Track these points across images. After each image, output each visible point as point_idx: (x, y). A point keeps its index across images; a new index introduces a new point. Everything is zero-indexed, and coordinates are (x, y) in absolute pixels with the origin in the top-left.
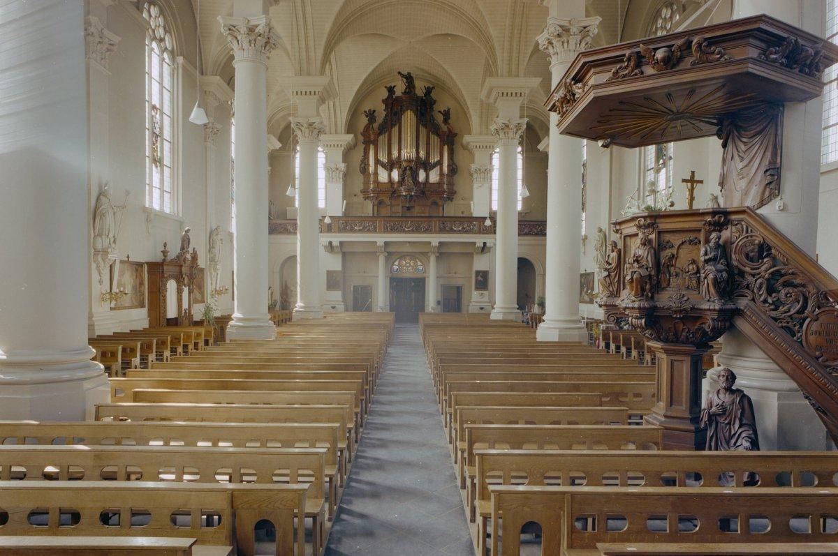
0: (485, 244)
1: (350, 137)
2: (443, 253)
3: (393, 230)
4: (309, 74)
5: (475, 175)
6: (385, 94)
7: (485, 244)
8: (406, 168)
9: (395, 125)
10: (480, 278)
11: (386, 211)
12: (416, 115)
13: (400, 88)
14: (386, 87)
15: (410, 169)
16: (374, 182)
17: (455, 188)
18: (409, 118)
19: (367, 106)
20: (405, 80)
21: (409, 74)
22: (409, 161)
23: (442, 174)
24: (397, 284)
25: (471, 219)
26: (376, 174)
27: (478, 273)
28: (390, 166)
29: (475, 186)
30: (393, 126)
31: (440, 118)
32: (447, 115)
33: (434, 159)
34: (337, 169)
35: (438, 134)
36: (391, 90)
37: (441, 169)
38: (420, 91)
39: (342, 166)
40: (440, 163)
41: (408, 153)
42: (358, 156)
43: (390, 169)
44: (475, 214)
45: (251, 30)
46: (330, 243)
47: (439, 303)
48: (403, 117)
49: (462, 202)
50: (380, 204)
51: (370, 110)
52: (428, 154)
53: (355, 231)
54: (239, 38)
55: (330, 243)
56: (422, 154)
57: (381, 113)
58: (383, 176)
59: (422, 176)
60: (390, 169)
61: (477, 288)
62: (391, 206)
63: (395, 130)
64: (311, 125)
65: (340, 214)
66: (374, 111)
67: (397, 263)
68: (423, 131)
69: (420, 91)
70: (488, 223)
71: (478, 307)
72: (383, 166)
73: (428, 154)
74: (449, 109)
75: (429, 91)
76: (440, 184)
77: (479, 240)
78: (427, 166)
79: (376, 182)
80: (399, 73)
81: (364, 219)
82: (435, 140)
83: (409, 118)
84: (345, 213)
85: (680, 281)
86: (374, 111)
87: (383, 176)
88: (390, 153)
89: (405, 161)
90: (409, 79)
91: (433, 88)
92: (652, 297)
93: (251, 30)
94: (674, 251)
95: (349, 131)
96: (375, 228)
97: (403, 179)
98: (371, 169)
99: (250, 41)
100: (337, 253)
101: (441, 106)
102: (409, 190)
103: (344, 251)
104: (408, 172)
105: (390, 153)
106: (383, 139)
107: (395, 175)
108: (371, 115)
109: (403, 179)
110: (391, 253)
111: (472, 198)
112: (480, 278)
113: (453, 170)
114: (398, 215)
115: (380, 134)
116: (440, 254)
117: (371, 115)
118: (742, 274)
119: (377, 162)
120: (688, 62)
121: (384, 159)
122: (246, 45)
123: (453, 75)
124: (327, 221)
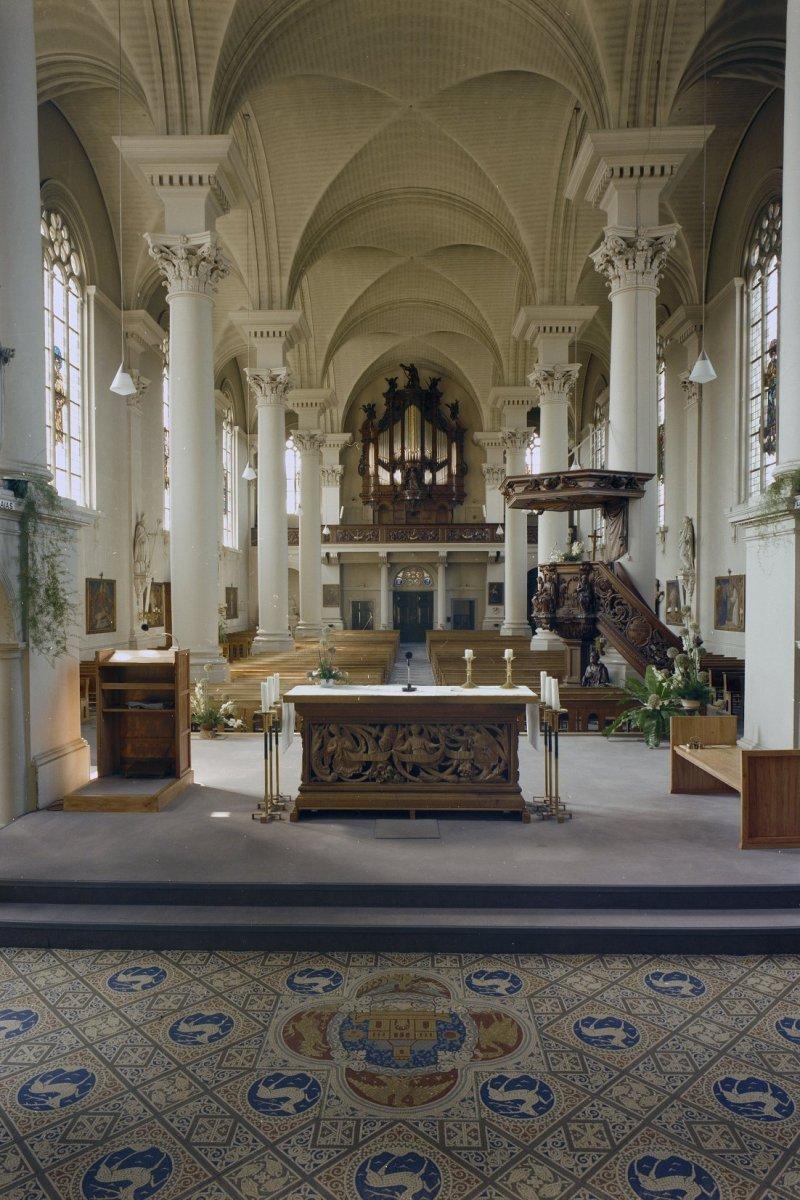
0: (498, 553)
1: (347, 436)
2: (452, 563)
3: (397, 539)
4: (311, 387)
5: (487, 476)
6: (386, 387)
7: (498, 553)
8: (410, 469)
9: (397, 421)
10: (494, 591)
11: (388, 518)
12: (421, 410)
13: (402, 381)
14: (387, 379)
15: (414, 470)
16: (375, 485)
17: (465, 491)
18: (412, 413)
19: (365, 401)
20: (408, 372)
21: (412, 365)
22: (413, 461)
23: (450, 475)
24: (402, 600)
25: (483, 526)
26: (376, 476)
27: (492, 585)
28: (392, 467)
29: (488, 487)
30: (395, 421)
31: (448, 412)
32: (455, 408)
33: (441, 457)
34: (334, 471)
35: (445, 431)
36: (392, 383)
37: (450, 469)
38: (425, 377)
39: (339, 468)
40: (448, 462)
41: (412, 452)
42: (355, 457)
43: (392, 472)
44: (488, 521)
45: (273, 379)
46: (328, 554)
47: (448, 619)
48: (406, 412)
49: (473, 505)
50: (381, 509)
51: (369, 405)
52: (434, 453)
53: (356, 541)
54: (262, 385)
55: (328, 554)
56: (428, 453)
57: (382, 408)
58: (384, 477)
59: (428, 477)
60: (392, 472)
61: (491, 603)
62: (394, 511)
63: (397, 428)
64: (312, 437)
65: (338, 523)
66: (374, 405)
67: (401, 574)
68: (428, 427)
69: (424, 384)
70: (499, 531)
71: (492, 624)
72: (385, 467)
73: (434, 453)
74: (457, 403)
75: (434, 382)
76: (447, 486)
77: (491, 549)
78: (434, 467)
79: (377, 484)
80: (402, 365)
81: (363, 528)
82: (441, 436)
83: (412, 413)
84: (341, 520)
85: (569, 602)
86: (374, 405)
87: (384, 477)
88: (392, 453)
89: (408, 461)
90: (412, 371)
91: (439, 379)
92: (554, 611)
93: (273, 379)
94: (566, 585)
95: (346, 429)
96: (377, 537)
97: (407, 482)
98: (372, 470)
99: (272, 389)
100: (335, 565)
101: (449, 399)
102: (414, 494)
103: (343, 564)
104: (412, 474)
105: (392, 453)
106: (384, 436)
107: (398, 476)
108: (370, 410)
109: (407, 482)
110: (393, 564)
111: (484, 502)
112: (494, 591)
113: (463, 469)
114: (401, 522)
115: (381, 431)
116: (449, 564)
117: (370, 410)
118: (599, 598)
119: (378, 462)
120: (559, 487)
121: (384, 456)
122: (268, 392)
123: (461, 367)
124: (326, 531)
